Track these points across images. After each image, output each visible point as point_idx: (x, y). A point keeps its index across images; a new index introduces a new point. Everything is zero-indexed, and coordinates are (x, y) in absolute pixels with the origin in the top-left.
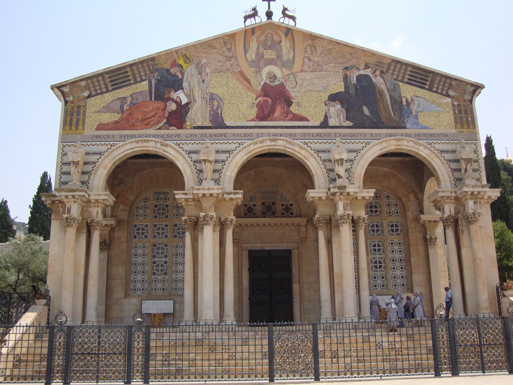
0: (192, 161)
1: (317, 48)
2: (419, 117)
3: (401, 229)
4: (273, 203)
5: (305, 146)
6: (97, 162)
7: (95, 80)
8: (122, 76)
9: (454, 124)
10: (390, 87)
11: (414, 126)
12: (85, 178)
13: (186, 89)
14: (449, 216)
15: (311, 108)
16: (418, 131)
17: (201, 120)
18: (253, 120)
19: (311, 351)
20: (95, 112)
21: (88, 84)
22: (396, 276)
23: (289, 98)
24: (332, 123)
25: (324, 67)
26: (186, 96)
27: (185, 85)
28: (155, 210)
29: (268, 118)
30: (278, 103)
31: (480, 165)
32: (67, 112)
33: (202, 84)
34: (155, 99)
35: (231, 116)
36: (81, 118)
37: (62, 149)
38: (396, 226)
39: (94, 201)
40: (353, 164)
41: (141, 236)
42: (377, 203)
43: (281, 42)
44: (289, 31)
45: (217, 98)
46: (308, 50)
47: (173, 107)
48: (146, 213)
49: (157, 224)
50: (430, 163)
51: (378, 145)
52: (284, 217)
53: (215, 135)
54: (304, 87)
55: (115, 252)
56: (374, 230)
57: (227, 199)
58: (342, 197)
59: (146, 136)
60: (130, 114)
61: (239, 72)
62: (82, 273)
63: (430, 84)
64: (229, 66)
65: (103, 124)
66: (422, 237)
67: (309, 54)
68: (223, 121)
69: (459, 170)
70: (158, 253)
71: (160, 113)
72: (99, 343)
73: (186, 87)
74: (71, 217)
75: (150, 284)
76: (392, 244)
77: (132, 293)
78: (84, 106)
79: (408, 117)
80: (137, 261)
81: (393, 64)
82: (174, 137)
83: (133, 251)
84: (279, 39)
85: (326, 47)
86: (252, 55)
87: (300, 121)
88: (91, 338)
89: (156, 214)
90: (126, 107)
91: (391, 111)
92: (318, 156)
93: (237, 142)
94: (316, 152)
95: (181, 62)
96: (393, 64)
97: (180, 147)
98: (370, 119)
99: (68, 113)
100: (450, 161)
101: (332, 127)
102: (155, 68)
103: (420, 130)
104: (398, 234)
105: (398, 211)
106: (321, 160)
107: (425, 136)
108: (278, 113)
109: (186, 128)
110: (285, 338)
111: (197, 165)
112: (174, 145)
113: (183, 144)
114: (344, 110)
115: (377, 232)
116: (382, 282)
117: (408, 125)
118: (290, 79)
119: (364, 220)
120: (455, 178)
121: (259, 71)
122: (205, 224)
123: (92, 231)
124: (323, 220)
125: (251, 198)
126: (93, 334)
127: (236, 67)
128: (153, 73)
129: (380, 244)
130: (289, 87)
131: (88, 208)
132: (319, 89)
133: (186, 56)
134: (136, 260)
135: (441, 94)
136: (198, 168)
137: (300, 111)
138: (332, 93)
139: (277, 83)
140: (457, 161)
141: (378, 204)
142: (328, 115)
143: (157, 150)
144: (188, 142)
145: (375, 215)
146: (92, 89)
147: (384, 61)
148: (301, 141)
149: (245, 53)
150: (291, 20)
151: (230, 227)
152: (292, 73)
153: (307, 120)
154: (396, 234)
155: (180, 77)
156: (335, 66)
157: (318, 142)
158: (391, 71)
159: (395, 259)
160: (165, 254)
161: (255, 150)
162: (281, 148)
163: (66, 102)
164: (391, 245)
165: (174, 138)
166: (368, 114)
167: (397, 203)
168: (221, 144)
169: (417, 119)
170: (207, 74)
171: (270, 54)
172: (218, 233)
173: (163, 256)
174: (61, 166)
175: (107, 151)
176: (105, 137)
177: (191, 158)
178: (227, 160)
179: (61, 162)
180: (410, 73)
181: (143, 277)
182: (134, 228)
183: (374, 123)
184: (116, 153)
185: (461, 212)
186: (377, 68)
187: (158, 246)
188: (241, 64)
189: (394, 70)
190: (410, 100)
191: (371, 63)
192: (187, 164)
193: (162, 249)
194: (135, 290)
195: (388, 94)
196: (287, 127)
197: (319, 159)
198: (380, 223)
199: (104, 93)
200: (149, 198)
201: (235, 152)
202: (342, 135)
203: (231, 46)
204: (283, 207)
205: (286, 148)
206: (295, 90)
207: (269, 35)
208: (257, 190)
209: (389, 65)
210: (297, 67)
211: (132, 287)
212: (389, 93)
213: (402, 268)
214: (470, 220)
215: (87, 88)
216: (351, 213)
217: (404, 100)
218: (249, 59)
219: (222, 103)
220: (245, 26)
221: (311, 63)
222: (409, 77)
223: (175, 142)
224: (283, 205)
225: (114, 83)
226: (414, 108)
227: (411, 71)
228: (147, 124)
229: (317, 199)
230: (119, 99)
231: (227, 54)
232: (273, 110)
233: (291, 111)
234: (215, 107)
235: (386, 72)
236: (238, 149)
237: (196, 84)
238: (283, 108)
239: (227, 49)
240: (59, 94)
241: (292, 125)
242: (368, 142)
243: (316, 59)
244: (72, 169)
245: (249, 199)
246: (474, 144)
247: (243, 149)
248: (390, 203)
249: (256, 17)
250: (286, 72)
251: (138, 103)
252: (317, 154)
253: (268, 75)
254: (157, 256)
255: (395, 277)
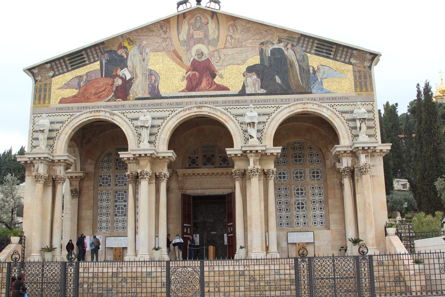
0: (134, 126)
1: (239, 28)
2: (323, 83)
3: (321, 175)
4: (213, 156)
5: (226, 112)
6: (60, 129)
7: (57, 62)
8: (80, 58)
9: (354, 88)
10: (299, 58)
11: (319, 91)
12: (51, 142)
13: (130, 66)
14: (346, 167)
15: (231, 79)
16: (322, 95)
17: (142, 93)
18: (183, 91)
19: (198, 282)
20: (58, 89)
21: (52, 66)
22: (316, 215)
23: (214, 71)
24: (249, 92)
25: (243, 43)
26: (130, 73)
27: (129, 63)
28: (116, 163)
29: (196, 88)
30: (204, 76)
31: (376, 123)
32: (36, 89)
33: (142, 62)
34: (105, 77)
35: (166, 88)
36: (48, 94)
37: (33, 119)
38: (317, 173)
39: (57, 161)
40: (265, 125)
41: (105, 185)
42: (301, 154)
43: (208, 23)
44: (214, 14)
45: (154, 74)
46: (231, 29)
47: (119, 82)
48: (110, 165)
49: (118, 174)
50: (332, 122)
51: (287, 109)
52: (222, 167)
53: (153, 105)
54: (226, 62)
55: (84, 198)
56: (298, 176)
57: (160, 158)
58: (253, 155)
59: (98, 107)
60: (86, 90)
61: (173, 50)
62: (49, 218)
63: (334, 54)
64: (165, 46)
65: (65, 98)
66: (338, 182)
67: (231, 33)
68: (159, 93)
69: (355, 128)
70: (119, 198)
71: (109, 87)
72: (43, 275)
73: (130, 65)
74: (38, 175)
75: (112, 224)
76: (313, 188)
77: (98, 231)
78: (49, 84)
79: (314, 83)
80: (102, 205)
81: (302, 38)
82: (120, 107)
83: (99, 197)
84: (206, 21)
85: (245, 26)
86: (183, 36)
87: (222, 90)
88: (37, 271)
89: (118, 167)
90: (82, 84)
91: (299, 79)
92: (236, 120)
93: (170, 110)
94: (235, 116)
95: (126, 44)
96: (302, 38)
97: (124, 116)
98: (281, 87)
99: (38, 90)
100: (349, 120)
101: (249, 95)
102: (105, 50)
103: (323, 94)
104: (319, 180)
105: (319, 160)
106: (239, 123)
107: (328, 99)
108: (204, 84)
109: (129, 100)
110: (179, 272)
111: (138, 129)
112: (120, 114)
113: (127, 113)
114: (259, 80)
115: (300, 178)
116: (304, 220)
117: (314, 91)
118: (215, 55)
119: (273, 172)
120: (352, 134)
121: (189, 50)
122: (142, 178)
123: (56, 184)
124: (239, 173)
125: (195, 151)
126: (38, 268)
127: (171, 47)
128: (103, 54)
129: (303, 188)
130: (213, 62)
131: (53, 166)
132: (239, 63)
133: (130, 39)
134: (101, 204)
135: (344, 62)
136: (138, 132)
137: (223, 82)
138: (250, 65)
139: (204, 59)
140: (354, 120)
141: (302, 154)
142: (246, 85)
143: (107, 118)
144: (131, 111)
145: (299, 164)
146: (56, 70)
147: (294, 36)
148: (222, 107)
149: (178, 34)
150: (217, 4)
151: (164, 180)
152: (216, 50)
153: (227, 89)
154: (317, 180)
155: (125, 57)
156: (253, 42)
157: (236, 108)
158: (301, 44)
159: (315, 201)
160: (125, 199)
161: (184, 116)
162: (206, 113)
163: (36, 81)
164: (312, 189)
165: (120, 108)
166: (279, 82)
167: (318, 153)
168: (158, 112)
169: (322, 84)
170: (147, 53)
171: (198, 34)
172: (154, 185)
173: (123, 200)
174: (32, 133)
175: (67, 120)
176: (66, 109)
177: (133, 124)
178: (162, 125)
179: (32, 130)
180: (317, 45)
181: (107, 218)
182: (99, 178)
183: (285, 90)
184: (74, 122)
185: (357, 163)
186: (289, 42)
187: (119, 193)
188: (174, 44)
189: (303, 43)
190: (316, 69)
191: (283, 38)
192: (130, 130)
193: (122, 195)
194: (101, 228)
195: (297, 64)
196: (211, 96)
197: (237, 122)
198: (303, 170)
199: (65, 72)
200: (111, 154)
201: (168, 119)
202: (257, 101)
203: (167, 29)
204: (221, 159)
205: (210, 113)
206: (218, 64)
207: (198, 18)
208: (199, 145)
209: (299, 39)
210: (220, 44)
211: (99, 226)
212: (298, 64)
213: (321, 208)
214: (363, 171)
215: (52, 68)
216: (259, 167)
217: (311, 69)
218: (181, 39)
219: (159, 77)
220: (178, 12)
221: (233, 41)
222: (316, 49)
223: (121, 111)
224: (221, 157)
225: (73, 64)
226: (319, 75)
227: (317, 44)
228: (99, 97)
229: (234, 155)
230: (77, 77)
231: (163, 36)
232: (200, 82)
233: (214, 82)
234: (153, 81)
235: (297, 45)
236: (171, 116)
237: (138, 62)
238: (209, 80)
239: (163, 32)
240: (31, 74)
241: (215, 94)
242: (279, 106)
243: (237, 37)
244: (41, 136)
245: (193, 152)
246: (372, 105)
247: (175, 115)
248: (312, 153)
249: (187, 3)
250: (212, 49)
251: (92, 80)
252: (236, 118)
253: (196, 53)
254: (118, 201)
255: (315, 216)
